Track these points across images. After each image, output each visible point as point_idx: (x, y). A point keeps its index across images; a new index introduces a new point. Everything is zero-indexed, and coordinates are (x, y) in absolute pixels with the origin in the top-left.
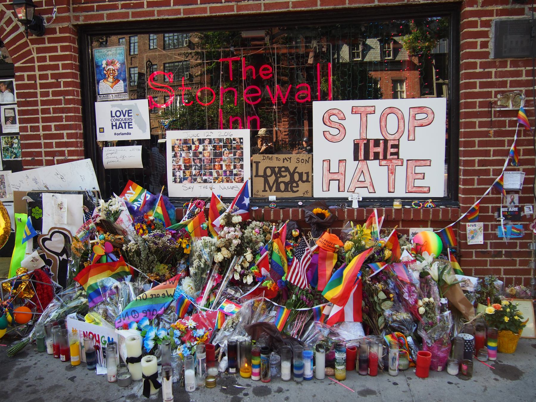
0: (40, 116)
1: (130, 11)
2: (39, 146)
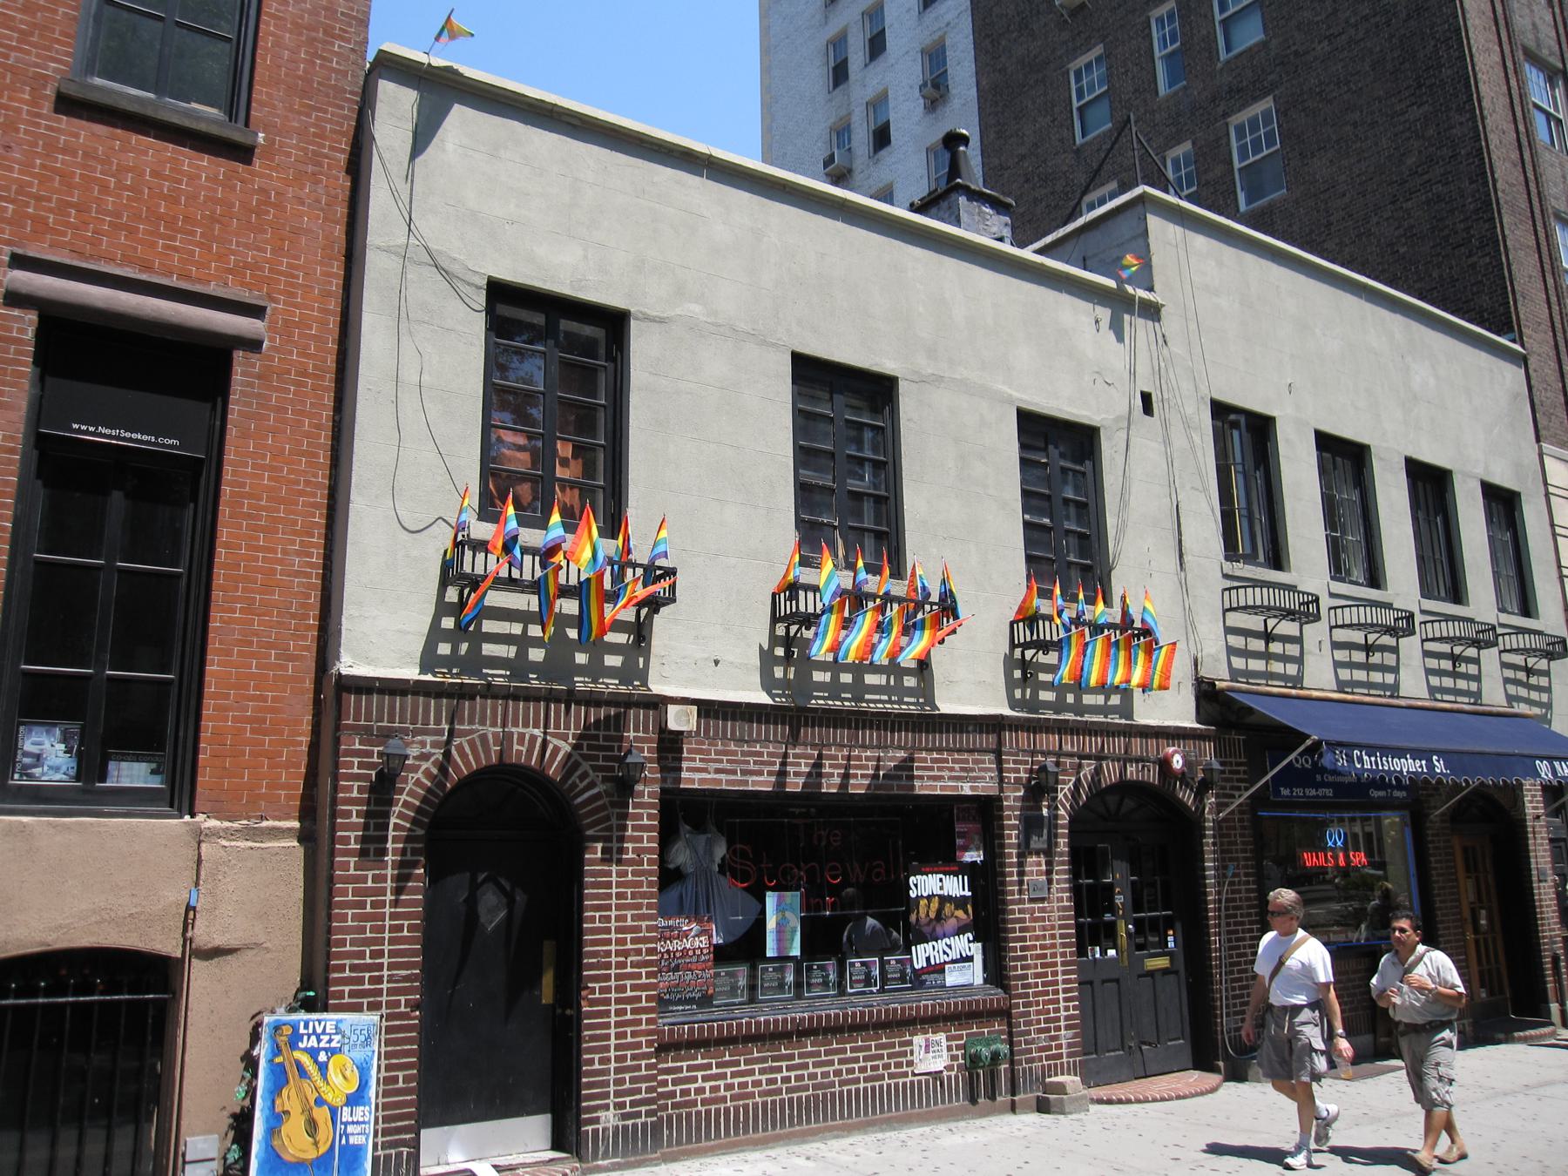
0: (614, 901)
1: (723, 776)
2: (609, 942)
